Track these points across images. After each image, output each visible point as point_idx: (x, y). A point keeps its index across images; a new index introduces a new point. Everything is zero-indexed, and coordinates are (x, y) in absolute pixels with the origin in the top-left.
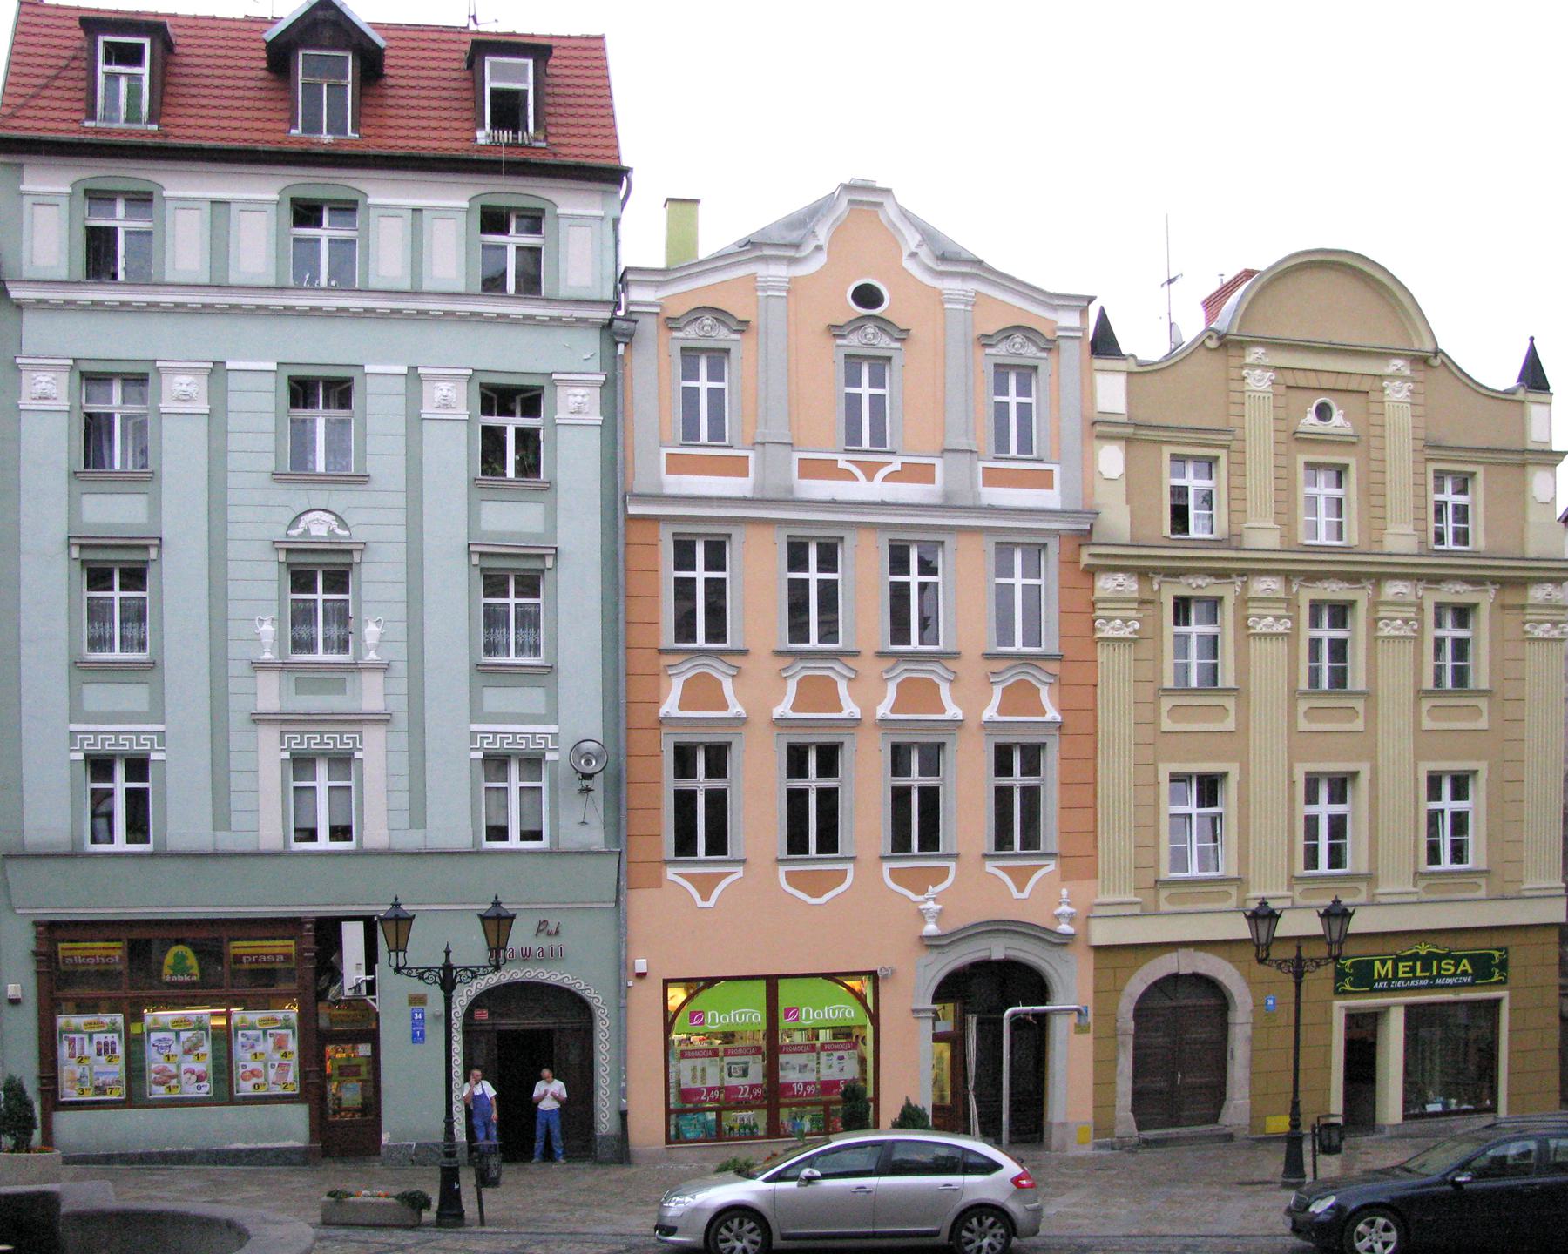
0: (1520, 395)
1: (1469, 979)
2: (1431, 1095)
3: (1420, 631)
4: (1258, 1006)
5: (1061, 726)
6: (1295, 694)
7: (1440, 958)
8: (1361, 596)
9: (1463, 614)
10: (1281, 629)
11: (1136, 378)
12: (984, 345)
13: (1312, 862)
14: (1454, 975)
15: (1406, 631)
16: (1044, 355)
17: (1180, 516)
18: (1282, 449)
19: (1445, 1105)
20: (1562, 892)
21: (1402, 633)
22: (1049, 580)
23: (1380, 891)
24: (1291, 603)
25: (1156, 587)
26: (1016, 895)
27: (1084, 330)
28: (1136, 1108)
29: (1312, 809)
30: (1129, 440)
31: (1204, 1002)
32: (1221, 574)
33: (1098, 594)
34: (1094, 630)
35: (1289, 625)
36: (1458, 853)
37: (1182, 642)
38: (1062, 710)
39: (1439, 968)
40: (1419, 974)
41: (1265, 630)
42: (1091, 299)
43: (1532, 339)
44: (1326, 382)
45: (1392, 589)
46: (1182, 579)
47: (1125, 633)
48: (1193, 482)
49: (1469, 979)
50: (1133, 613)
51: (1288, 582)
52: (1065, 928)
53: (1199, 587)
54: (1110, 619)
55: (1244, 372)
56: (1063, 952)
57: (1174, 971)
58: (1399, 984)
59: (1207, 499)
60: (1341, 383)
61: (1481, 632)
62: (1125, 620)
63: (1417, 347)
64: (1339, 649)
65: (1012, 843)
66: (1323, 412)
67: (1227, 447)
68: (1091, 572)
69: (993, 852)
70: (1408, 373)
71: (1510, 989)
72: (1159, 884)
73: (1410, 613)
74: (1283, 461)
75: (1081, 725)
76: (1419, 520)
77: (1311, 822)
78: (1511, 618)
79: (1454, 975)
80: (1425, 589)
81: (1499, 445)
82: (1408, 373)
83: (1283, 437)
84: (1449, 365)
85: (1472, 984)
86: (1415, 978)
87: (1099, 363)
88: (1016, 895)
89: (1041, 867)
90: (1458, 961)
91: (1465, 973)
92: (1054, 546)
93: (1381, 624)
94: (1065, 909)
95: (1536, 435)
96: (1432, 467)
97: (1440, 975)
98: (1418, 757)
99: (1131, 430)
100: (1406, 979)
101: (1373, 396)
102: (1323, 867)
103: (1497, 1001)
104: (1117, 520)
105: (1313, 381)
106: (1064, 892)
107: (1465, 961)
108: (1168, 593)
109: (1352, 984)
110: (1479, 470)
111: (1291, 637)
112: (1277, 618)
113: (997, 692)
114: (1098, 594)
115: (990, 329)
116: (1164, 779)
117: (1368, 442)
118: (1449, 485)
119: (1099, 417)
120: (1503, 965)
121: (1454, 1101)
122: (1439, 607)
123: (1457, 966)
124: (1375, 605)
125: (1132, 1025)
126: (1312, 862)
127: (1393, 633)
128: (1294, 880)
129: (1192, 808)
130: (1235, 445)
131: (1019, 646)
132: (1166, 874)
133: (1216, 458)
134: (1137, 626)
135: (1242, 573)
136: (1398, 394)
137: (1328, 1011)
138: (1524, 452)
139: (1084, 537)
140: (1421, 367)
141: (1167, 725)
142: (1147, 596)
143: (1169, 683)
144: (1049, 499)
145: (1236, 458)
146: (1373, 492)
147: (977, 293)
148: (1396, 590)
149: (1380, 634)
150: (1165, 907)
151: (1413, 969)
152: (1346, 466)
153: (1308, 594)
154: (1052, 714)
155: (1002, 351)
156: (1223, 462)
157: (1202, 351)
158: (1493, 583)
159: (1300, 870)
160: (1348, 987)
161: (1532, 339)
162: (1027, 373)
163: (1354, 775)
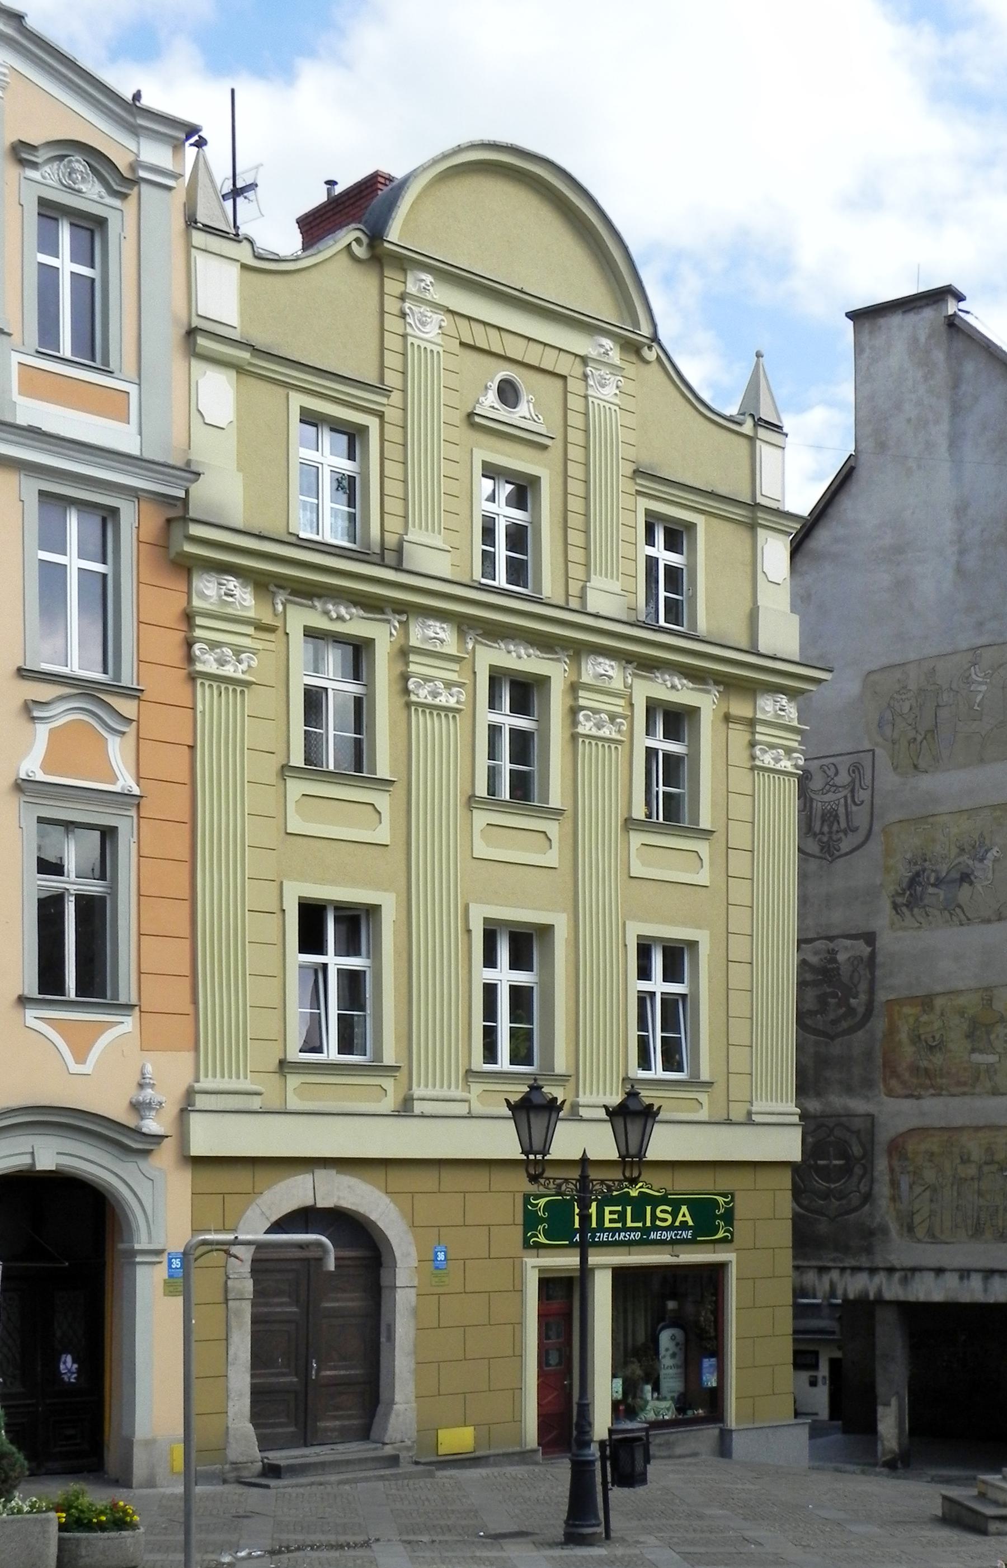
1: (688, 1234)
4: (427, 1260)
6: (472, 801)
7: (655, 1202)
8: (555, 671)
9: (676, 720)
10: (452, 702)
12: (23, 163)
13: (490, 1053)
20: (796, 1119)
26: (74, 1068)
28: (256, 1417)
29: (490, 975)
32: (372, 606)
40: (629, 1224)
44: (515, 349)
49: (688, 1234)
51: (462, 634)
57: (309, 1202)
60: (533, 355)
64: (523, 745)
67: (381, 415)
72: (284, 1066)
77: (490, 991)
80: (635, 675)
88: (74, 1068)
96: (644, 504)
99: (246, 355)
100: (614, 1231)
104: (224, 492)
107: (684, 1209)
120: (729, 1217)
122: (652, 707)
123: (674, 1215)
125: (248, 1285)
126: (490, 1053)
130: (392, 415)
135: (402, 608)
140: (633, 358)
142: (268, 619)
150: (294, 1103)
153: (491, 655)
158: (717, 683)
159: (478, 1064)
160: (542, 1239)
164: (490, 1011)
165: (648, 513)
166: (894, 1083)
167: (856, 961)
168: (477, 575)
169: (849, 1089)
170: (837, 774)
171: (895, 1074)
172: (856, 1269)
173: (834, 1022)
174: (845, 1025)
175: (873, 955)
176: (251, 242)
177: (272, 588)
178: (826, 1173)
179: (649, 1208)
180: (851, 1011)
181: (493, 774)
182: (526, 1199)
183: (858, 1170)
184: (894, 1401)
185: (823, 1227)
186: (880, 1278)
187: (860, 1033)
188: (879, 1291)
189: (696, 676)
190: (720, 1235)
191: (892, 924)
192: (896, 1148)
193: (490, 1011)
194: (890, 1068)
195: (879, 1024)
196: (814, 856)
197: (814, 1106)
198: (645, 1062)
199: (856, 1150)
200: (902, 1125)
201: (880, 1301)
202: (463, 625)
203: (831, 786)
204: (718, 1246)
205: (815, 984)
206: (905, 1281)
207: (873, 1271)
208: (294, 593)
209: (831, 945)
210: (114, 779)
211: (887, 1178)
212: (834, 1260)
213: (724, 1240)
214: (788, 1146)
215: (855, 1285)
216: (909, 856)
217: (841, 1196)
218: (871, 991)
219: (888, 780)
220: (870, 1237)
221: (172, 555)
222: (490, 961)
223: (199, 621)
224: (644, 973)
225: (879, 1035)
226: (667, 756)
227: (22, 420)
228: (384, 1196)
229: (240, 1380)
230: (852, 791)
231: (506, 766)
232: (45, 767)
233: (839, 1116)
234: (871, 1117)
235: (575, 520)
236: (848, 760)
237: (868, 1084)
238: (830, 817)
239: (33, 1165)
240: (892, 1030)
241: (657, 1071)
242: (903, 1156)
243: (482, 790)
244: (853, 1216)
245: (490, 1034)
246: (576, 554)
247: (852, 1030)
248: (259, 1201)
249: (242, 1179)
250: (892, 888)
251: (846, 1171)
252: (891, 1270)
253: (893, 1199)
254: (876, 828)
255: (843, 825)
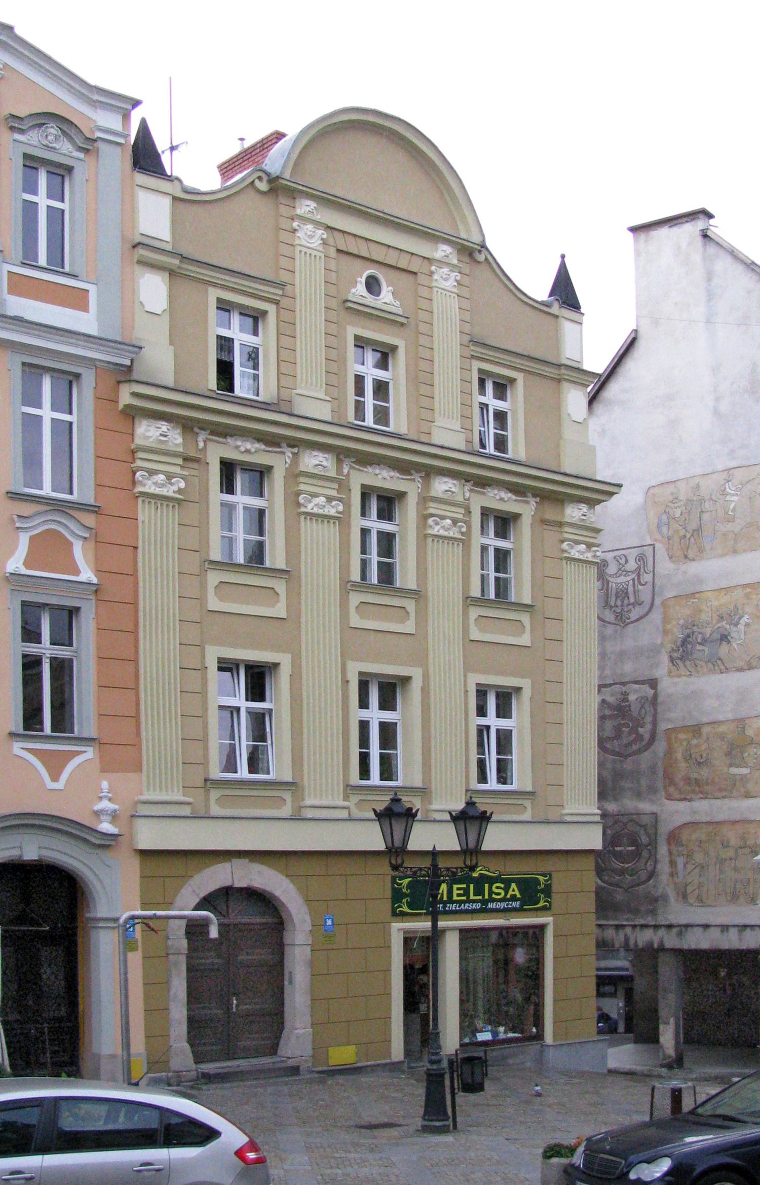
0: (555, 309)
1: (516, 904)
2: (479, 1024)
3: (468, 534)
5: (97, 590)
6: (347, 586)
7: (491, 881)
8: (411, 487)
10: (332, 512)
11: (181, 206)
12: (12, 128)
13: (365, 772)
14: (503, 900)
15: (453, 533)
16: (81, 155)
17: (225, 370)
18: (333, 316)
19: (495, 1034)
20: (598, 818)
21: (451, 534)
22: (83, 414)
23: (433, 807)
24: (343, 485)
25: (201, 445)
26: (51, 785)
27: (127, 136)
29: (364, 714)
30: (173, 273)
31: (258, 920)
32: (272, 442)
33: (138, 441)
34: (134, 483)
35: (341, 508)
36: (503, 774)
37: (229, 508)
38: (98, 571)
39: (491, 892)
40: (472, 897)
41: (315, 510)
42: (136, 103)
43: (563, 257)
45: (441, 486)
46: (229, 440)
47: (169, 491)
48: (239, 333)
49: (516, 904)
50: (177, 470)
51: (339, 462)
52: (106, 827)
53: (247, 451)
54: (152, 473)
55: (295, 224)
56: (106, 855)
58: (453, 907)
59: (253, 357)
60: (392, 258)
61: (523, 542)
62: (169, 477)
63: (463, 235)
64: (387, 542)
65: (41, 722)
66: (372, 285)
67: (277, 303)
68: (131, 414)
69: (21, 731)
70: (455, 262)
71: (553, 915)
72: (209, 783)
73: (459, 513)
74: (333, 329)
75: (119, 590)
76: (466, 417)
77: (364, 726)
78: (550, 535)
79: (503, 900)
81: (537, 355)
82: (455, 262)
83: (334, 304)
84: (492, 265)
85: (520, 910)
86: (469, 901)
87: (141, 178)
88: (51, 785)
89: (78, 753)
90: (507, 883)
91: (514, 898)
92: (89, 378)
93: (430, 521)
94: (105, 804)
95: (568, 353)
96: (476, 365)
97: (493, 900)
98: (468, 668)
101: (422, 279)
102: (375, 778)
103: (542, 927)
104: (160, 360)
105: (363, 249)
106: (105, 784)
107: (513, 885)
108: (217, 452)
109: (410, 906)
110: (519, 377)
111: (342, 520)
112: (330, 499)
113: (24, 540)
114: (138, 441)
115: (22, 112)
116: (212, 665)
117: (417, 326)
118: (489, 387)
119: (138, 239)
120: (547, 891)
121: (502, 1029)
122: (485, 513)
123: (506, 890)
124: (424, 500)
125: (185, 943)
126: (365, 772)
127: (442, 533)
128: (350, 789)
129: (240, 700)
130: (284, 302)
131: (47, 490)
132: (216, 773)
133: (264, 313)
134: (182, 485)
135: (293, 443)
136: (445, 280)
137: (387, 934)
138: (560, 366)
139: (125, 374)
141: (214, 603)
142: (192, 453)
143: (216, 554)
144: (85, 322)
145: (285, 315)
146: (421, 381)
147: (6, 65)
148: (445, 487)
149: (430, 532)
150: (215, 810)
151: (466, 892)
152: (394, 348)
153: (360, 477)
154: (87, 575)
155: (33, 141)
156: (272, 318)
157: (251, 193)
158: (534, 496)
159: (355, 778)
160: (406, 909)
161: (563, 257)
162: (61, 172)
163: (406, 680)
164: (364, 741)
165: (480, 371)
166: (671, 789)
167: (643, 700)
168: (351, 417)
169: (639, 795)
170: (627, 561)
171: (672, 782)
172: (643, 926)
173: (626, 746)
174: (635, 747)
175: (655, 696)
176: (178, 179)
177: (196, 430)
178: (619, 856)
179: (487, 885)
180: (640, 738)
181: (364, 564)
182: (393, 881)
183: (645, 854)
184: (672, 1021)
185: (619, 896)
186: (661, 932)
187: (646, 753)
188: (661, 943)
189: (518, 491)
190: (541, 904)
191: (670, 672)
192: (673, 837)
193: (364, 741)
194: (669, 779)
195: (660, 746)
196: (609, 623)
197: (612, 807)
198: (483, 778)
199: (644, 839)
200: (679, 821)
201: (662, 949)
202: (341, 454)
203: (622, 571)
204: (539, 913)
205: (611, 717)
206: (680, 934)
207: (656, 927)
208: (212, 433)
209: (624, 689)
210: (77, 572)
211: (667, 859)
212: (627, 920)
213: (544, 908)
214: (592, 839)
215: (644, 938)
216: (682, 622)
217: (633, 873)
218: (654, 723)
219: (664, 566)
220: (655, 902)
221: (121, 406)
222: (364, 704)
223: (140, 455)
224: (481, 711)
225: (661, 754)
226: (497, 550)
227: (10, 313)
228: (284, 878)
229: (179, 1012)
230: (639, 575)
231: (374, 558)
232: (27, 564)
233: (632, 814)
234: (655, 815)
236: (635, 552)
237: (652, 790)
238: (623, 593)
239: (21, 856)
240: (670, 751)
241: (493, 784)
242: (679, 843)
243: (356, 576)
244: (641, 887)
245: (364, 759)
247: (639, 751)
248: (191, 882)
249: (178, 866)
250: (669, 646)
251: (637, 855)
252: (670, 926)
253: (672, 875)
254: (657, 602)
255: (632, 600)
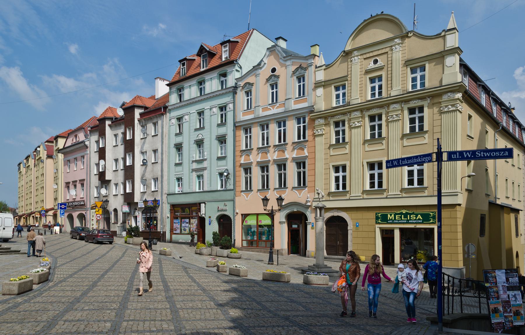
7: (410, 214)
39: (410, 217)
86: (402, 220)
97: (410, 220)
100: (399, 220)
107: (419, 216)
123: (416, 217)
151: (401, 217)
160: (380, 222)
235: (389, 79)
246: (389, 86)
